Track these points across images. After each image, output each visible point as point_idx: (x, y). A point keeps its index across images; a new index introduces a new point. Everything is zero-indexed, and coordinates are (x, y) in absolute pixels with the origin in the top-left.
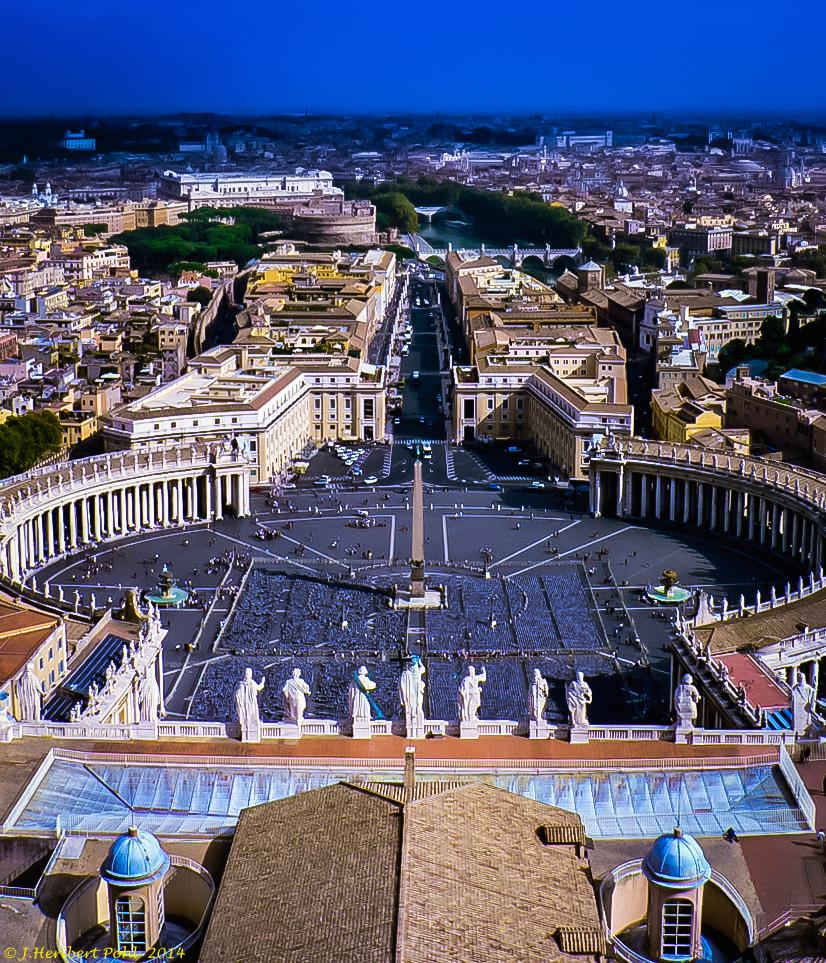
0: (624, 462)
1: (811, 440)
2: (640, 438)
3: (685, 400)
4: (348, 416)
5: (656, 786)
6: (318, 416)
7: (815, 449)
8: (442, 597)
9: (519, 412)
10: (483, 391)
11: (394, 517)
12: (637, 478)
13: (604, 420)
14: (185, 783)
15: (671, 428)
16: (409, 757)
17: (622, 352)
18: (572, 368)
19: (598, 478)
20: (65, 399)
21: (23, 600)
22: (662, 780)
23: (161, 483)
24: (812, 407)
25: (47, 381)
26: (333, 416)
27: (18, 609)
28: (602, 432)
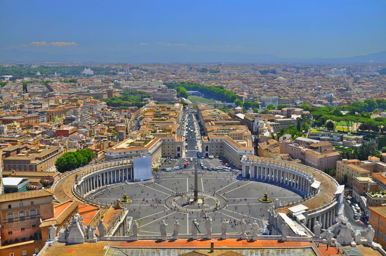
0: (252, 163)
1: (305, 157)
2: (256, 156)
3: (269, 145)
4: (173, 150)
5: (278, 252)
6: (164, 151)
7: (306, 160)
8: (203, 201)
9: (221, 149)
10: (211, 144)
11: (187, 179)
12: (256, 167)
13: (246, 151)
14: (147, 252)
15: (265, 153)
16: (212, 244)
17: (250, 132)
18: (235, 137)
19: (245, 167)
20: (92, 146)
21: (87, 203)
22: (279, 251)
23: (122, 169)
24: (306, 147)
25: (87, 141)
26: (168, 151)
27: (87, 206)
28: (245, 154)
